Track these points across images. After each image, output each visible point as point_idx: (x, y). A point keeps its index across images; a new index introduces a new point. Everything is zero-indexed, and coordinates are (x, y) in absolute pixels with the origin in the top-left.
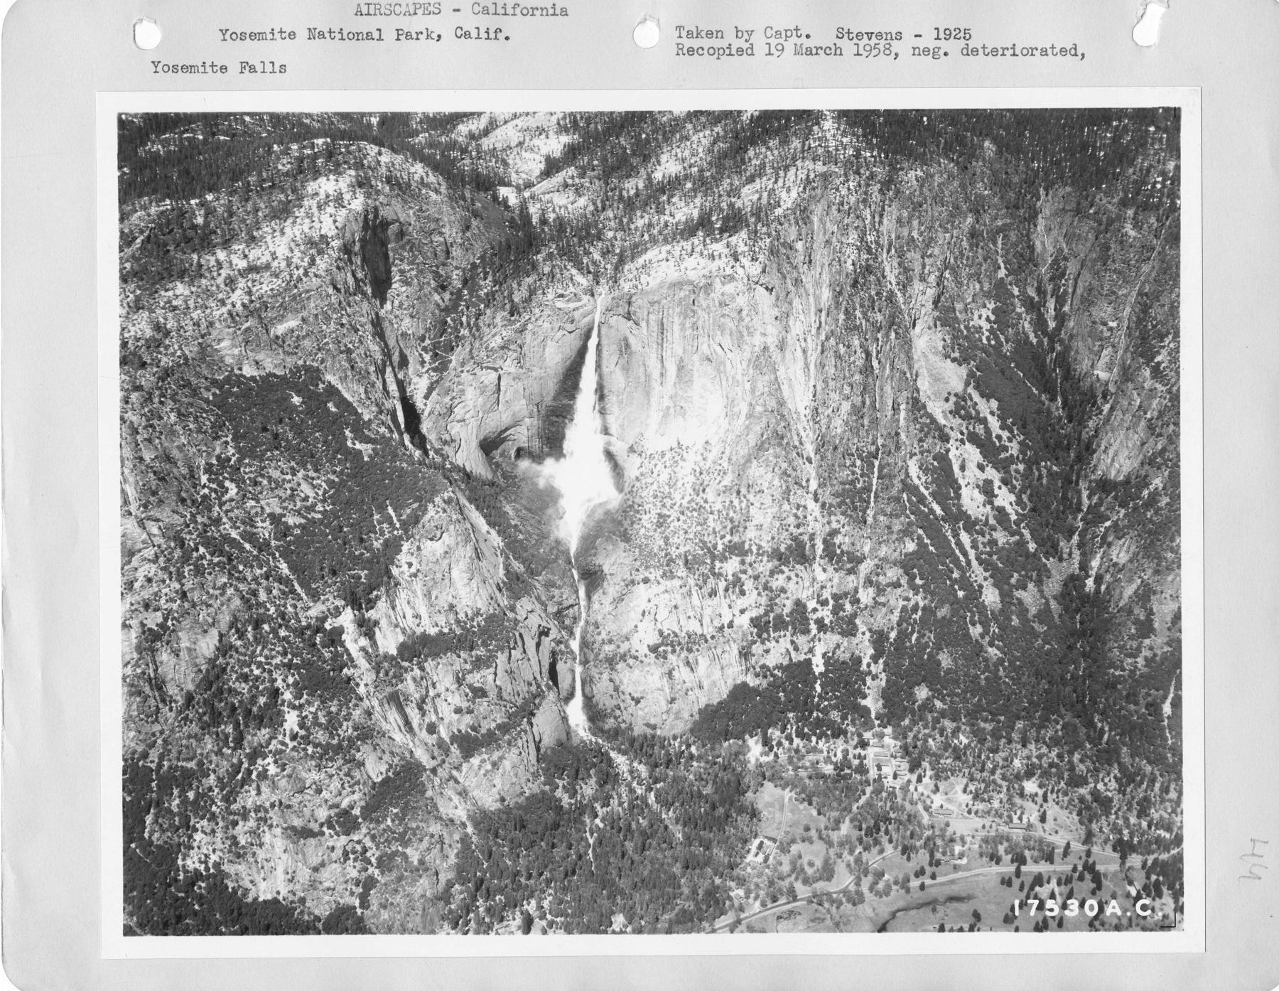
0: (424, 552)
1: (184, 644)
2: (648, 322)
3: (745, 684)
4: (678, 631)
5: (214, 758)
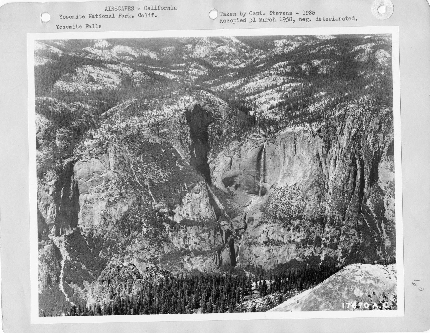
0: (193, 196)
1: (119, 207)
2: (280, 145)
3: (295, 259)
4: (274, 239)
5: (121, 238)
